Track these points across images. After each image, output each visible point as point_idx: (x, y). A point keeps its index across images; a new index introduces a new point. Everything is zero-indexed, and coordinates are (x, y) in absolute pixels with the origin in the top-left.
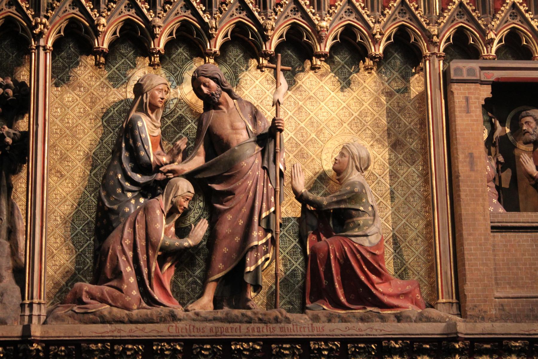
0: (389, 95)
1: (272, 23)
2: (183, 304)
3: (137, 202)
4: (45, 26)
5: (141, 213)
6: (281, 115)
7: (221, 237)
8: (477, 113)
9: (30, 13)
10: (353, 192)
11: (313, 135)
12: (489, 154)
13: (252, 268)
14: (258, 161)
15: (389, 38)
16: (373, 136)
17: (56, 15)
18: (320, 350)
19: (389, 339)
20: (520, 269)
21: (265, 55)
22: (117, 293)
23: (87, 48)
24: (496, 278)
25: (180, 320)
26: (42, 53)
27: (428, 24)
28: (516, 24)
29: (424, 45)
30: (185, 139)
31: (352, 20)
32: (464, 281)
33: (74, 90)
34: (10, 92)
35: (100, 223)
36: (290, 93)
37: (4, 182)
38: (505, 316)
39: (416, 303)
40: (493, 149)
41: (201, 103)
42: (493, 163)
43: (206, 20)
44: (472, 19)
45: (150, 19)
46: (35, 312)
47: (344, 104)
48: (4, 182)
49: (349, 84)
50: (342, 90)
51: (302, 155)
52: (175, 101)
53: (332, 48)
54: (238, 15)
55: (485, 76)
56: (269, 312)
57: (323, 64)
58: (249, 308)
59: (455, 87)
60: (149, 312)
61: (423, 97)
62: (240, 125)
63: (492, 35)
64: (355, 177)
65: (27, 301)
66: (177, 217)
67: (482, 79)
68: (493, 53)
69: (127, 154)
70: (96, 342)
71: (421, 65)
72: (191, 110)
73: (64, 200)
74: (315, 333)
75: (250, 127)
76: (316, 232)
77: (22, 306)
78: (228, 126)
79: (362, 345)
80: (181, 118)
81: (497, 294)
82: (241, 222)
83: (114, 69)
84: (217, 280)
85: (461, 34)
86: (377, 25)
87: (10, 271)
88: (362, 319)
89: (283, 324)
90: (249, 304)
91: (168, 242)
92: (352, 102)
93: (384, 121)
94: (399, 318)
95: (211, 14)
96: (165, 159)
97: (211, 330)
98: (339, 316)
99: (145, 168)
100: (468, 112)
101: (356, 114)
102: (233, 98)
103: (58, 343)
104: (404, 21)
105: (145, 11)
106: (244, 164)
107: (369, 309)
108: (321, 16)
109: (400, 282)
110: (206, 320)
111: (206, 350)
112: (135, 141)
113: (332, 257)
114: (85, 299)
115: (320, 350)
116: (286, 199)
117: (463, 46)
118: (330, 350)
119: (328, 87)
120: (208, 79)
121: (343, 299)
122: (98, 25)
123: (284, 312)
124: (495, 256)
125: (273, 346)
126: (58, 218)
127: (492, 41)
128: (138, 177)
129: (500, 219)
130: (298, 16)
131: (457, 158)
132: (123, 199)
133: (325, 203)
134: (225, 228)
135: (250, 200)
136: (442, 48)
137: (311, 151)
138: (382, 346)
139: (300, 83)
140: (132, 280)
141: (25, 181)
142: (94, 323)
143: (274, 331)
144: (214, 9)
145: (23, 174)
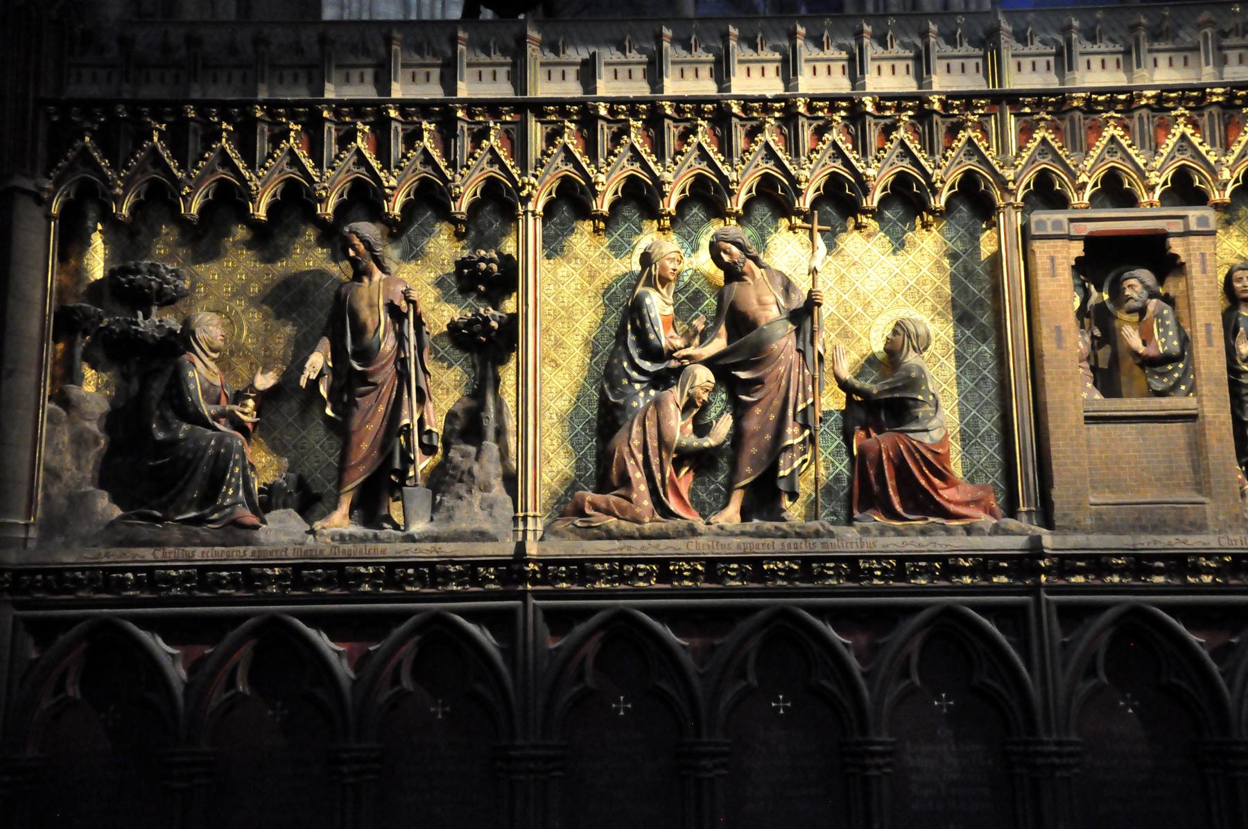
0: (953, 256)
1: (807, 173)
2: (704, 517)
3: (647, 395)
4: (533, 186)
5: (651, 408)
6: (820, 286)
7: (748, 435)
8: (1065, 276)
9: (515, 172)
10: (909, 377)
11: (859, 309)
12: (1082, 326)
13: (787, 472)
14: (791, 342)
15: (952, 187)
16: (934, 309)
17: (547, 173)
18: (871, 570)
20: (1123, 469)
21: (799, 213)
22: (625, 503)
23: (583, 211)
24: (1091, 481)
25: (701, 535)
26: (531, 219)
27: (1002, 167)
28: (1116, 161)
29: (997, 193)
30: (703, 318)
31: (906, 166)
32: (1051, 486)
33: (569, 262)
34: (495, 267)
35: (605, 419)
36: (829, 258)
37: (490, 374)
38: (1104, 527)
39: (992, 513)
40: (1086, 320)
41: (721, 274)
42: (1087, 339)
43: (726, 173)
44: (1058, 159)
45: (658, 174)
46: (530, 526)
47: (897, 271)
48: (490, 374)
49: (902, 245)
50: (894, 252)
51: (845, 334)
52: (690, 273)
53: (881, 201)
54: (765, 165)
55: (1076, 229)
56: (809, 524)
57: (871, 221)
58: (784, 520)
59: (1036, 245)
60: (663, 525)
61: (996, 259)
62: (770, 299)
63: (1083, 178)
64: (911, 358)
65: (520, 514)
66: (695, 412)
67: (1072, 233)
68: (1086, 200)
69: (634, 338)
70: (602, 561)
71: (994, 218)
72: (710, 283)
73: (561, 394)
74: (865, 549)
75: (782, 301)
76: (865, 428)
77: (515, 519)
78: (755, 302)
79: (923, 564)
80: (697, 292)
81: (1092, 500)
82: (772, 417)
83: (616, 235)
84: (743, 487)
86: (938, 171)
87: (500, 479)
88: (923, 532)
89: (825, 540)
90: (784, 515)
91: (684, 443)
92: (907, 267)
93: (947, 290)
94: (969, 530)
95: (732, 165)
96: (679, 342)
97: (738, 546)
98: (895, 529)
99: (654, 353)
100: (1054, 275)
102: (760, 266)
103: (558, 562)
104: (972, 164)
105: (651, 164)
106: (774, 346)
107: (931, 519)
108: (866, 163)
109: (969, 487)
110: (732, 534)
111: (733, 570)
112: (643, 322)
113: (884, 457)
114: (588, 511)
115: (871, 570)
116: (827, 388)
117: (1046, 193)
118: (884, 570)
119: (876, 250)
120: (729, 245)
121: (898, 508)
122: (597, 183)
123: (827, 524)
124: (1090, 452)
125: (814, 565)
126: (554, 416)
127: (1084, 185)
128: (647, 365)
129: (1096, 407)
130: (839, 163)
131: (1040, 333)
132: (629, 391)
133: (875, 392)
134: (752, 424)
135: (782, 391)
136: (1020, 197)
137: (856, 329)
138: (948, 565)
139: (842, 246)
140: (643, 488)
141: (514, 372)
142: (600, 538)
143: (815, 547)
144: (735, 159)
145: (512, 364)
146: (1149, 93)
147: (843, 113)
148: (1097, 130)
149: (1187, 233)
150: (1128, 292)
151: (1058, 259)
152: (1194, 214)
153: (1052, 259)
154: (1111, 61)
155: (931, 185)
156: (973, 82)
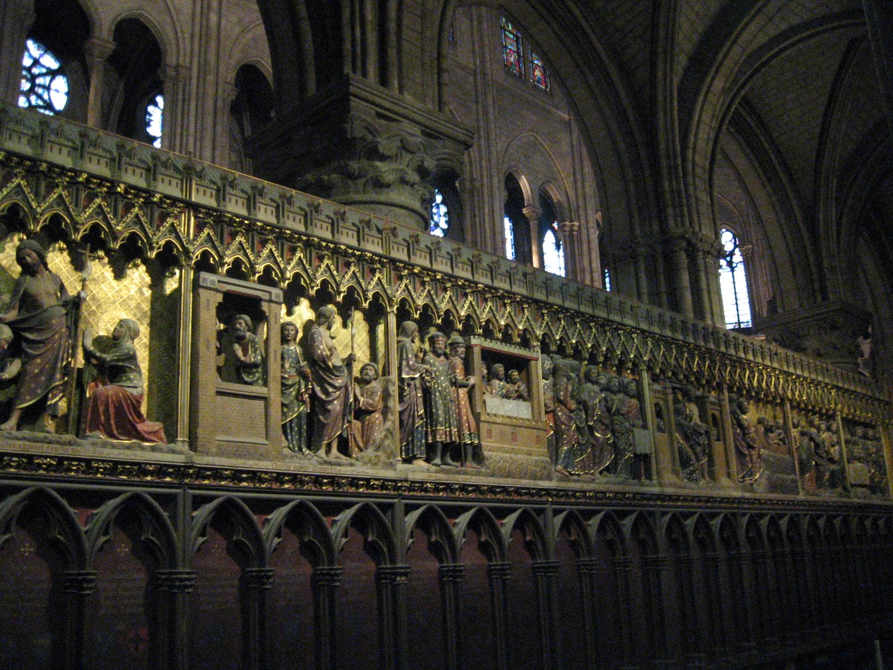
8: (213, 311)
11: (94, 308)
18: (98, 468)
19: (147, 464)
31: (136, 230)
38: (221, 453)
85: (205, 255)
94: (153, 449)
101: (125, 297)
121: (115, 432)
125: (66, 463)
133: (108, 359)
138: (140, 468)
146: (259, 224)
147: (105, 189)
148: (233, 235)
149: (270, 301)
150: (238, 326)
151: (211, 300)
152: (275, 291)
153: (208, 301)
154: (240, 201)
155: (151, 244)
156: (176, 193)
